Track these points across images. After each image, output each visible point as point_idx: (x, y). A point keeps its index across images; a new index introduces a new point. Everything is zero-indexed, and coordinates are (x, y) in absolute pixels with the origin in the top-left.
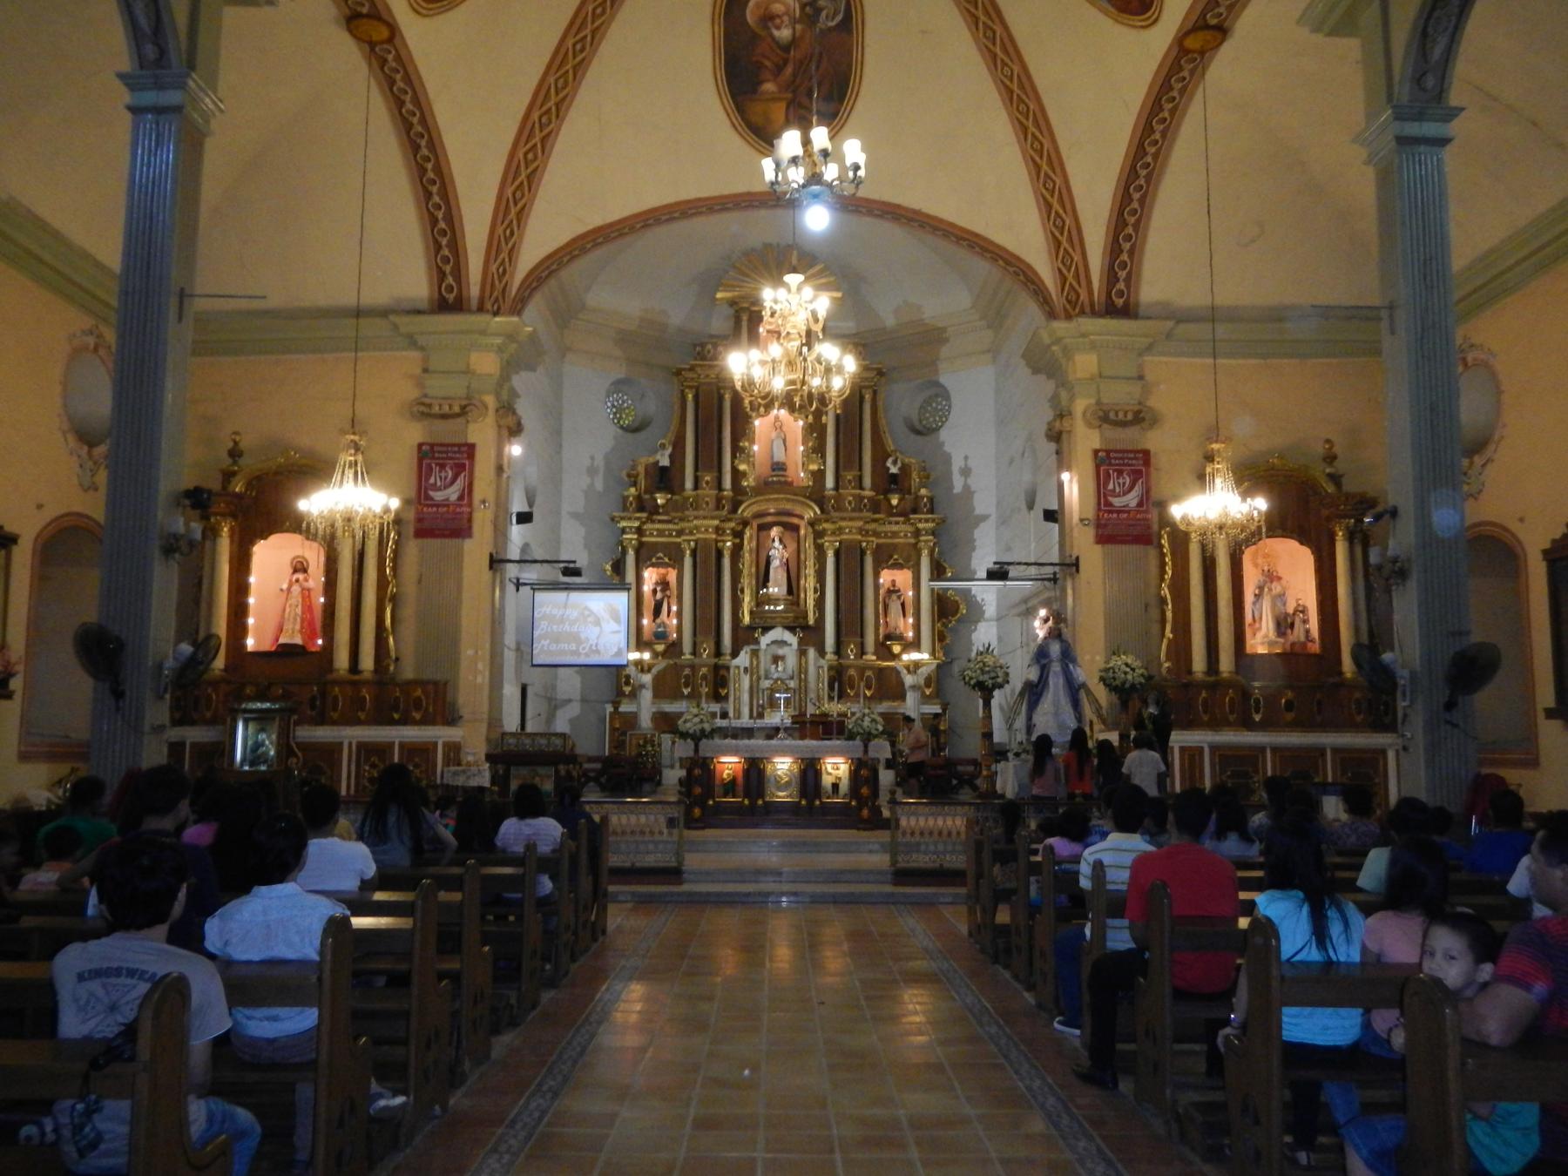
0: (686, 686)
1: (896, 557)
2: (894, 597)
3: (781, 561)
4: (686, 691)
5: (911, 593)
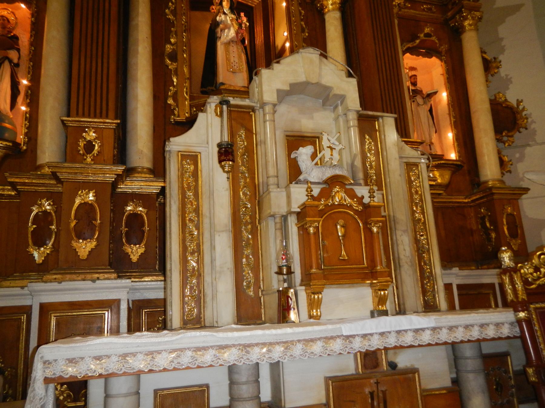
0: (39, 243)
1: (427, 30)
2: (419, 99)
3: (237, 33)
4: (38, 255)
5: (444, 95)
